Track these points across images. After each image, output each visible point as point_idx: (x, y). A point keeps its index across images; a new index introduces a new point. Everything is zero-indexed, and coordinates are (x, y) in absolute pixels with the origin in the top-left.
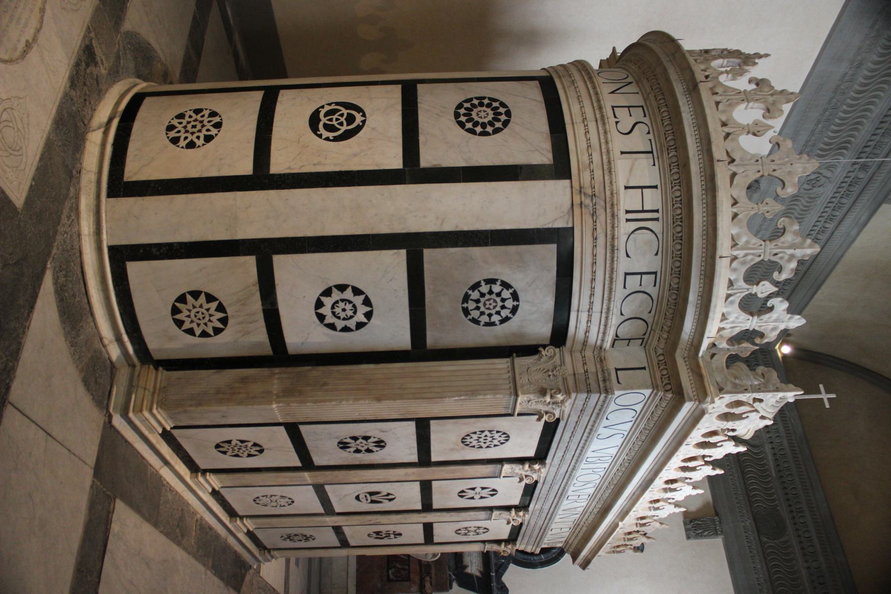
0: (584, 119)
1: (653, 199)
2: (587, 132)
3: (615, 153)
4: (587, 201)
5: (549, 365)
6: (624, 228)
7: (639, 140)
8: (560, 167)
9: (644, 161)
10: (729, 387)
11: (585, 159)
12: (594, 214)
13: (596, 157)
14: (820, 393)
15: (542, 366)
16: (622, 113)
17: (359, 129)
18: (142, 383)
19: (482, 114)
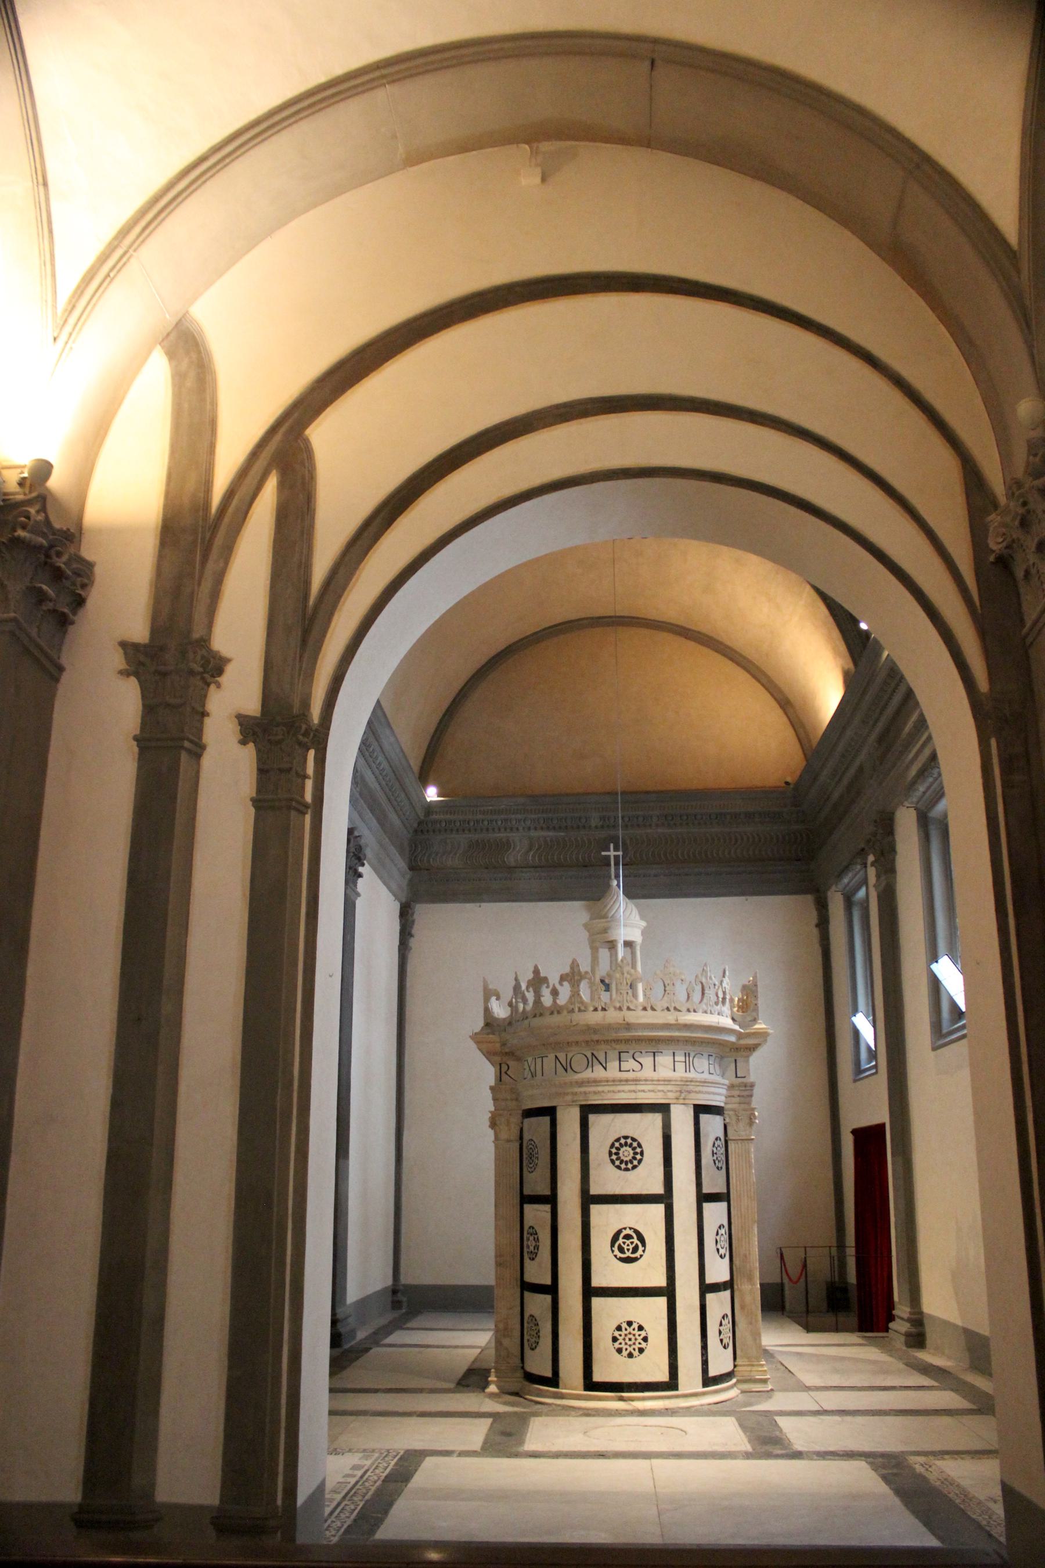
0: (634, 1091)
1: (680, 1058)
2: (643, 1091)
3: (655, 1076)
4: (683, 1095)
5: (734, 1118)
6: (692, 1075)
7: (647, 1061)
8: (663, 1109)
9: (659, 1059)
10: (754, 1014)
11: (660, 1095)
12: (689, 1092)
13: (660, 1088)
14: (609, 856)
15: (734, 1122)
16: (625, 1066)
18: (746, 1374)
19: (626, 1154)
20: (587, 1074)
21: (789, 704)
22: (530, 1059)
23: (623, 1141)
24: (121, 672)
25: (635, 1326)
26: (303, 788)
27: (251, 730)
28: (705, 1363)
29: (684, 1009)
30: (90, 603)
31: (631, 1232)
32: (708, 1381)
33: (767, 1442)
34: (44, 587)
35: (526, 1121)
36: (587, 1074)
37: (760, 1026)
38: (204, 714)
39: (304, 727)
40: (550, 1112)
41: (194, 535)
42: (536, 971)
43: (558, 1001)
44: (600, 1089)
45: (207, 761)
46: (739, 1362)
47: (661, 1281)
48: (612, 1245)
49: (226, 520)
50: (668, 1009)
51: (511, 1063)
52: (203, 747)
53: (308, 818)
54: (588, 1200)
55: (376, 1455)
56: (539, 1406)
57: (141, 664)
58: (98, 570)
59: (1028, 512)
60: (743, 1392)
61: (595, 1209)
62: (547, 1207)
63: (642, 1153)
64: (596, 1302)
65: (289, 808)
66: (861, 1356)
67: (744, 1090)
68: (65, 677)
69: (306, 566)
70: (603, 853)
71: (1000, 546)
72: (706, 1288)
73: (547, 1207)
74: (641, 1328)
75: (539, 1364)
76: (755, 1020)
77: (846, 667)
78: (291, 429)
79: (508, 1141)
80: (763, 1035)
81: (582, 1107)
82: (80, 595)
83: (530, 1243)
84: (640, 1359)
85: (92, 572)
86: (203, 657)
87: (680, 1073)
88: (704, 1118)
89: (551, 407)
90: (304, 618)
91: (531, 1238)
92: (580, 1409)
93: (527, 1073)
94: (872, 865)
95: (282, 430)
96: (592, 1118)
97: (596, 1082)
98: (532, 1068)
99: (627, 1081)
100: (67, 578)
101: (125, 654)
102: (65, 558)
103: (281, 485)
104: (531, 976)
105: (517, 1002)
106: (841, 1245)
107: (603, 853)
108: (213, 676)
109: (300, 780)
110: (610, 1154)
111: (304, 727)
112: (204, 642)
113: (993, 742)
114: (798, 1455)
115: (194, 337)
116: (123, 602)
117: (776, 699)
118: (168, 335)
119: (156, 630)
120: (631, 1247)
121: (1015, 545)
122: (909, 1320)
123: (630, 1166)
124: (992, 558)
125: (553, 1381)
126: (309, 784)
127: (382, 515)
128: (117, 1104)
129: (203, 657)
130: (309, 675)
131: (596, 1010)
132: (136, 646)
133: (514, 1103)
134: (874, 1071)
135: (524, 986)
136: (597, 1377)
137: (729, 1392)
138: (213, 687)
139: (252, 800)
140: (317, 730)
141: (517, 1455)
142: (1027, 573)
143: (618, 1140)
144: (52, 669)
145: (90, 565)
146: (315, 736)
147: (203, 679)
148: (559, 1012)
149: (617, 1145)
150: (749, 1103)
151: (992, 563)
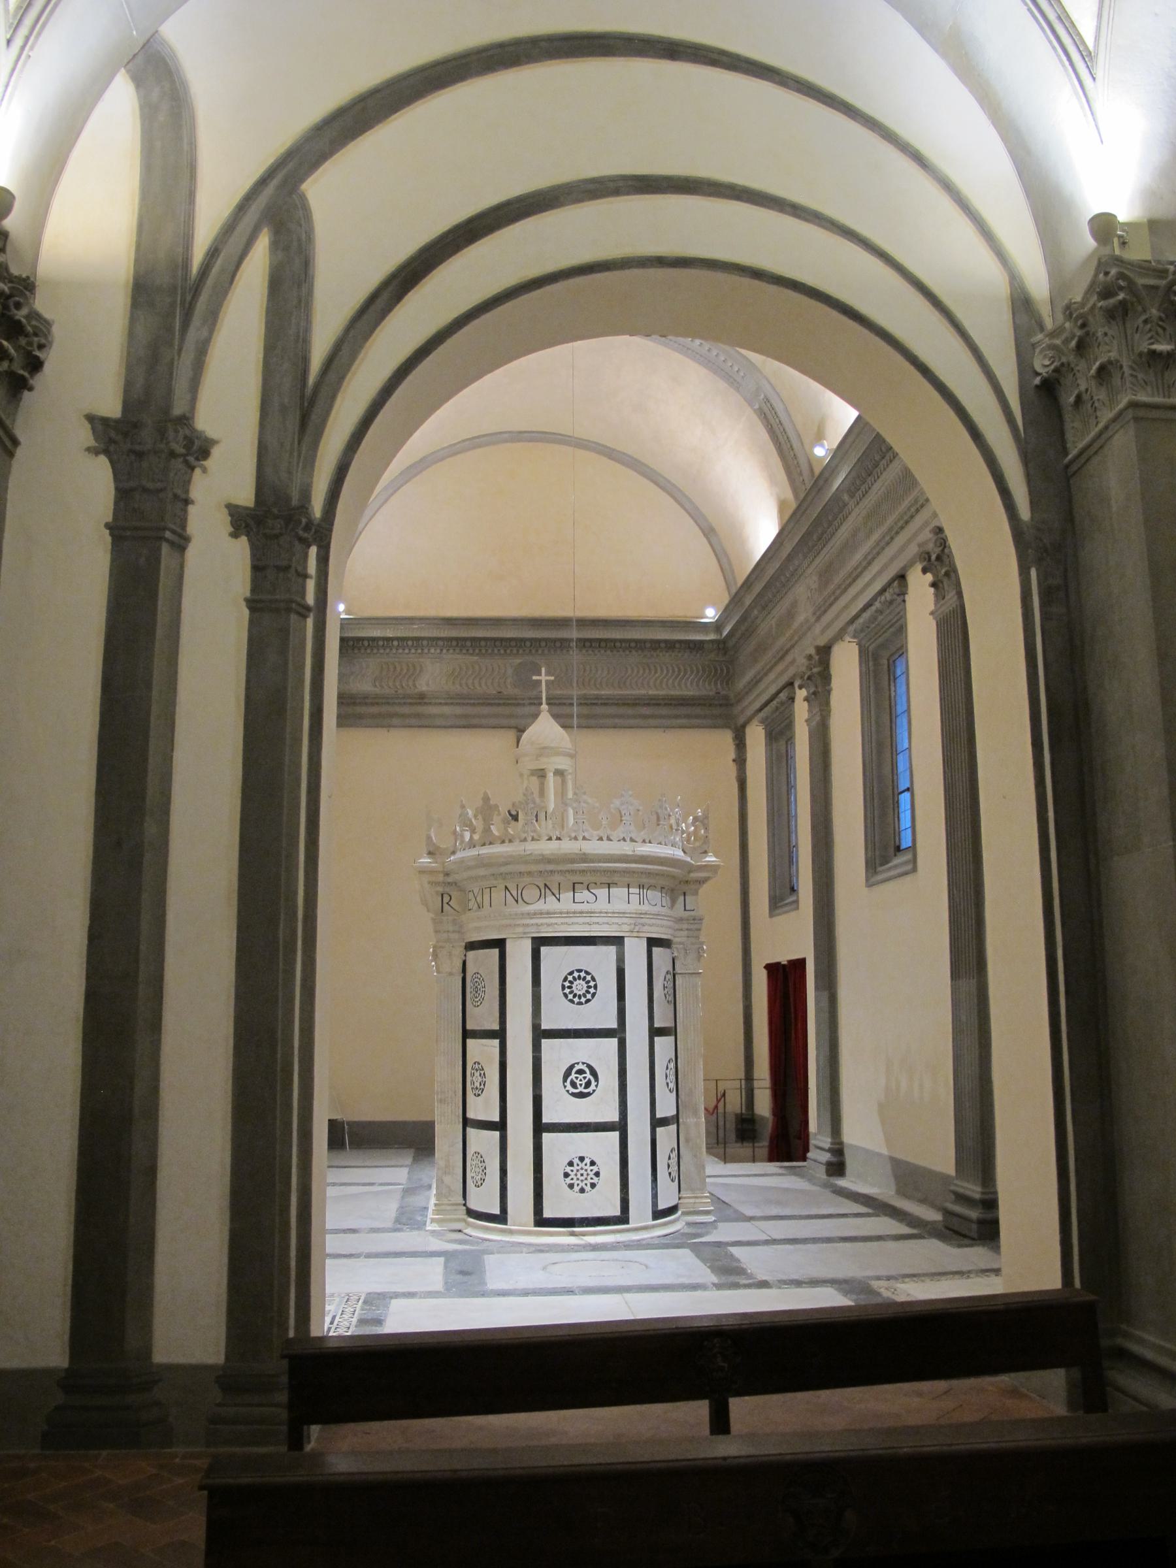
3: (609, 908)
6: (646, 908)
7: (602, 893)
11: (615, 927)
13: (616, 920)
17: (589, 1066)
19: (579, 987)
20: (540, 906)
21: (715, 534)
22: (476, 891)
23: (576, 974)
24: (88, 450)
25: (587, 1161)
26: (304, 587)
27: (243, 521)
28: (655, 1196)
29: (639, 839)
30: (47, 368)
31: (584, 1067)
32: (658, 1214)
33: (730, 1273)
34: (5, 343)
35: (471, 954)
36: (540, 906)
37: (711, 858)
38: (187, 502)
39: (304, 520)
40: (500, 944)
41: (170, 299)
42: (486, 799)
43: (510, 830)
44: (553, 921)
45: (191, 552)
46: (683, 1194)
47: (614, 1117)
48: (565, 1080)
49: (210, 282)
50: (624, 840)
51: (454, 894)
52: (187, 539)
53: (310, 622)
54: (540, 1034)
55: (337, 1299)
56: (487, 1243)
57: (111, 441)
58: (55, 330)
59: (1087, 334)
60: (688, 1224)
61: (545, 1043)
62: (496, 1042)
63: (595, 987)
64: (546, 1137)
65: (289, 610)
66: (786, 1185)
67: (694, 923)
68: (20, 453)
69: (303, 341)
70: (534, 678)
71: (1047, 370)
72: (657, 1123)
73: (496, 1042)
74: (593, 1163)
75: (485, 1199)
76: (705, 852)
77: (782, 497)
78: (285, 182)
79: (451, 974)
80: (713, 868)
81: (533, 939)
82: (37, 358)
83: (473, 1079)
84: (591, 1194)
85: (49, 331)
86: (186, 437)
87: (634, 906)
88: (656, 951)
89: (580, 181)
90: (302, 397)
91: (477, 1074)
92: (530, 1245)
93: (472, 904)
94: (806, 699)
95: (275, 183)
96: (544, 950)
97: (549, 913)
98: (479, 899)
99: (581, 913)
100: (27, 335)
101: (93, 429)
102: (24, 311)
103: (275, 245)
104: (480, 803)
105: (462, 831)
106: (749, 1077)
107: (534, 678)
108: (197, 459)
109: (300, 580)
110: (563, 987)
111: (304, 520)
112: (185, 420)
113: (1033, 573)
114: (764, 1284)
115: (166, 64)
116: (86, 371)
117: (701, 528)
118: (134, 56)
119: (128, 405)
120: (584, 1082)
121: (1064, 369)
122: (829, 1150)
123: (583, 1000)
124: (1037, 381)
125: (502, 1218)
126: (311, 585)
127: (390, 288)
128: (95, 937)
129: (186, 437)
130: (309, 462)
131: (550, 839)
132: (105, 421)
133: (456, 936)
134: (794, 906)
135: (470, 813)
136: (547, 1214)
137: (676, 1225)
138: (198, 471)
139: (247, 600)
140: (319, 525)
141: (484, 1294)
142: (1079, 400)
143: (571, 973)
144: (8, 443)
145: (48, 324)
146: (316, 532)
147: (186, 462)
148: (510, 841)
149: (570, 978)
150: (697, 937)
151: (1037, 386)
